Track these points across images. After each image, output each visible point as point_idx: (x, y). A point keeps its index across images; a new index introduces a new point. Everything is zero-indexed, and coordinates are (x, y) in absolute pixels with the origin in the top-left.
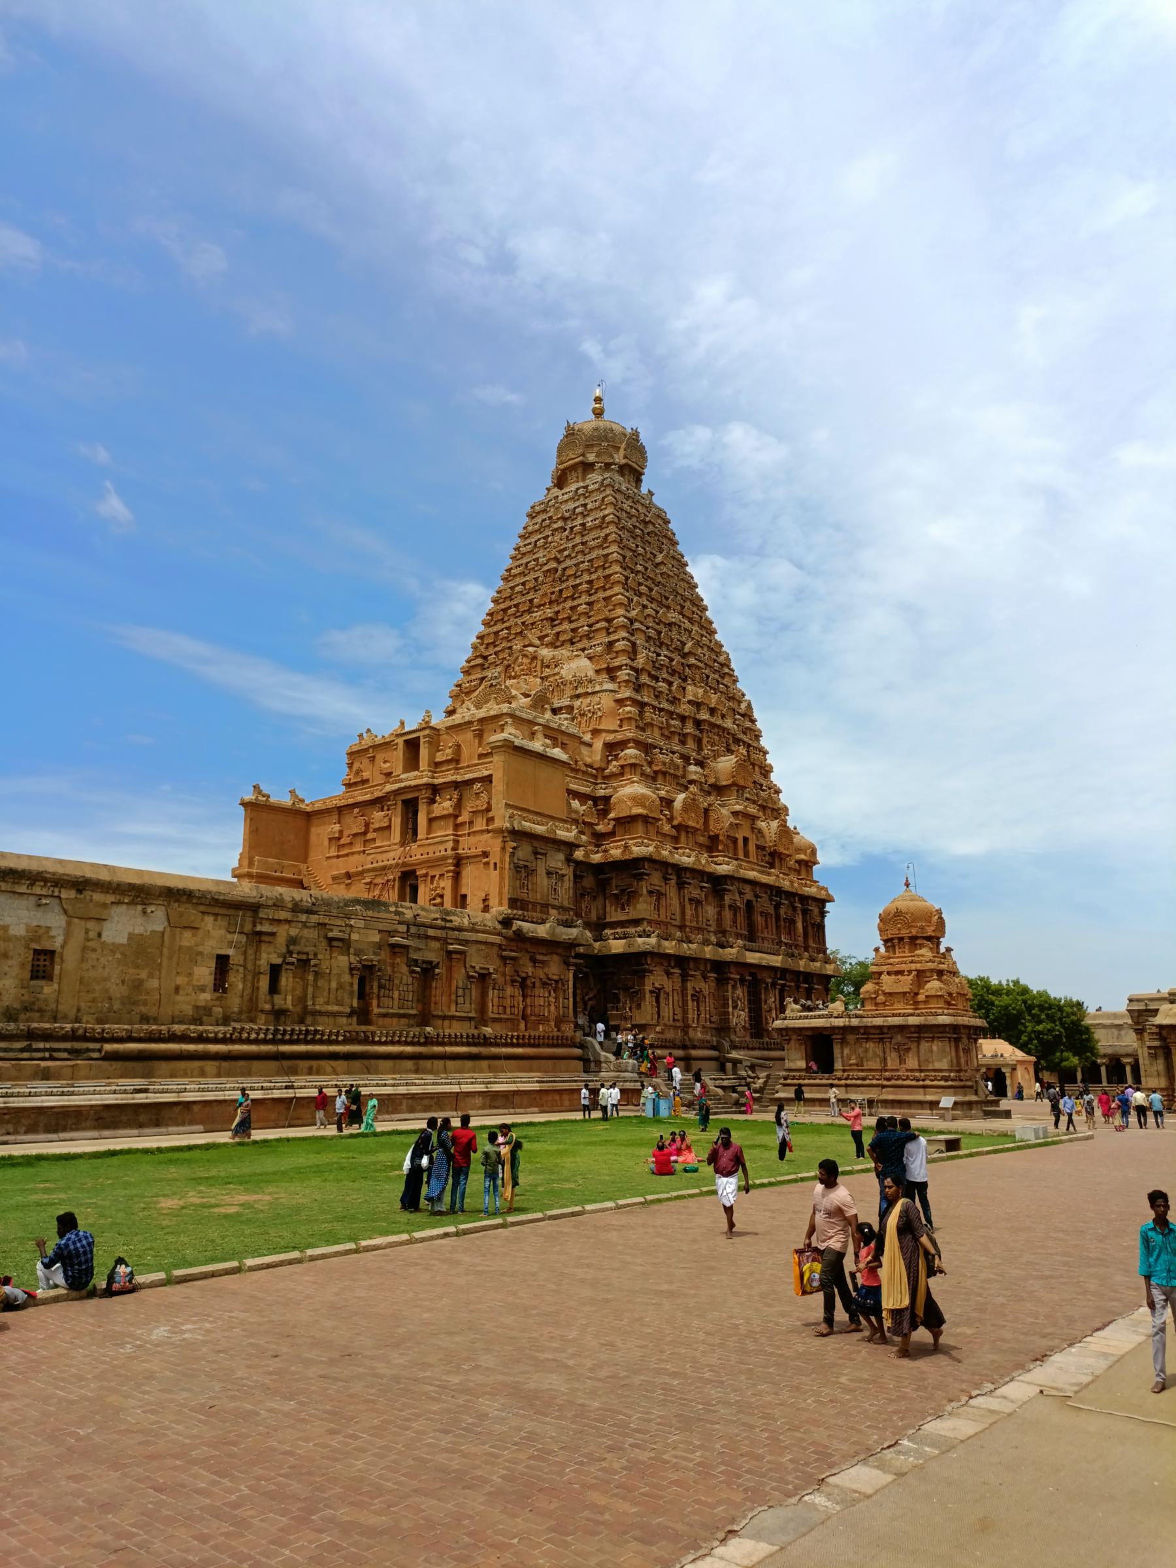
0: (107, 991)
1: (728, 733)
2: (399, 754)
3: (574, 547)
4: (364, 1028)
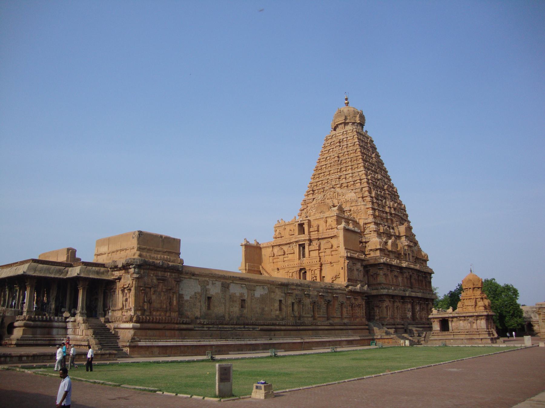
2: (297, 228)
3: (344, 152)
4: (315, 321)
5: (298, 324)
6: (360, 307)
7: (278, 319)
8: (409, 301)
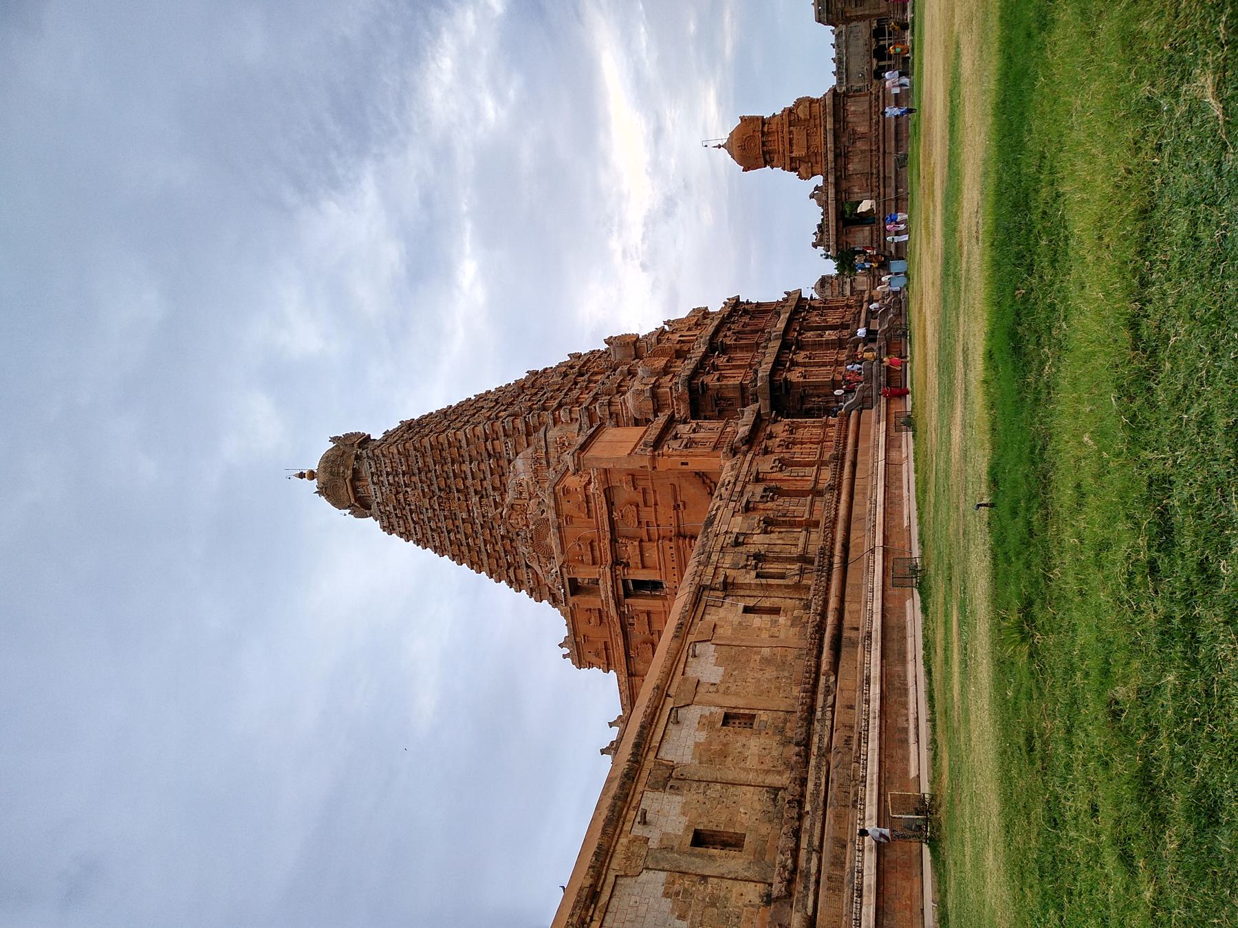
0: (769, 680)
2: (584, 601)
3: (421, 481)
4: (822, 524)
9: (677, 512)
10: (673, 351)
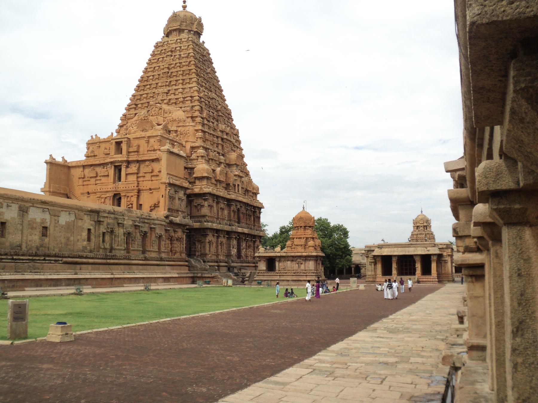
0: (60, 241)
1: (232, 143)
2: (113, 147)
3: (176, 64)
4: (128, 255)
5: (108, 257)
6: (180, 241)
7: (85, 251)
8: (235, 237)
9: (148, 190)
10: (229, 182)
